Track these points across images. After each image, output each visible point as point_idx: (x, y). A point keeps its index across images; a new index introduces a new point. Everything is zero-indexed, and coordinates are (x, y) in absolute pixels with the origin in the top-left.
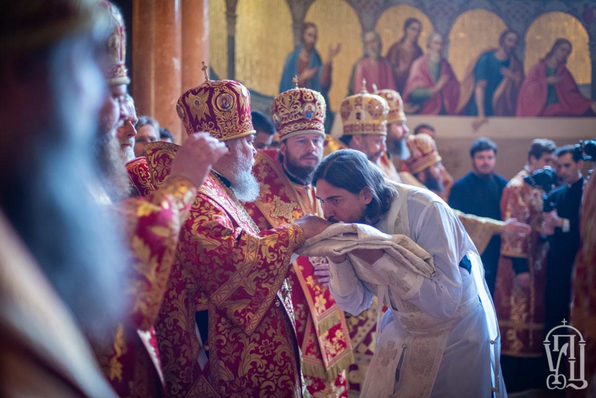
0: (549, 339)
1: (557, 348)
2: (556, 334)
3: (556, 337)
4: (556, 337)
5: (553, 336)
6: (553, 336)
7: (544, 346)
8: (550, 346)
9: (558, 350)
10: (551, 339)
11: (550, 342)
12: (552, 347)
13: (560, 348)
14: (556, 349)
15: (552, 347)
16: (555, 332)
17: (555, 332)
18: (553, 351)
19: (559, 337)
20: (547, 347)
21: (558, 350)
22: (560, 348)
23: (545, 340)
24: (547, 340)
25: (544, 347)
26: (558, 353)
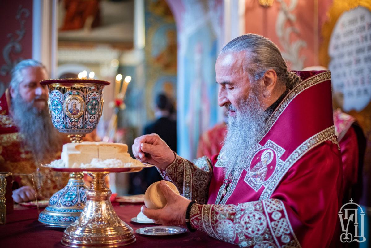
0: (342, 211)
1: (347, 217)
2: (346, 208)
3: (346, 210)
4: (346, 210)
5: (345, 209)
6: (345, 209)
7: (339, 215)
8: (342, 216)
9: (347, 218)
10: (343, 211)
11: (342, 213)
12: (343, 216)
13: (348, 217)
14: (346, 217)
15: (343, 216)
16: (346, 207)
17: (346, 207)
18: (344, 218)
19: (348, 210)
20: (341, 216)
21: (347, 218)
22: (348, 217)
23: (339, 211)
24: (340, 212)
25: (338, 216)
26: (347, 220)
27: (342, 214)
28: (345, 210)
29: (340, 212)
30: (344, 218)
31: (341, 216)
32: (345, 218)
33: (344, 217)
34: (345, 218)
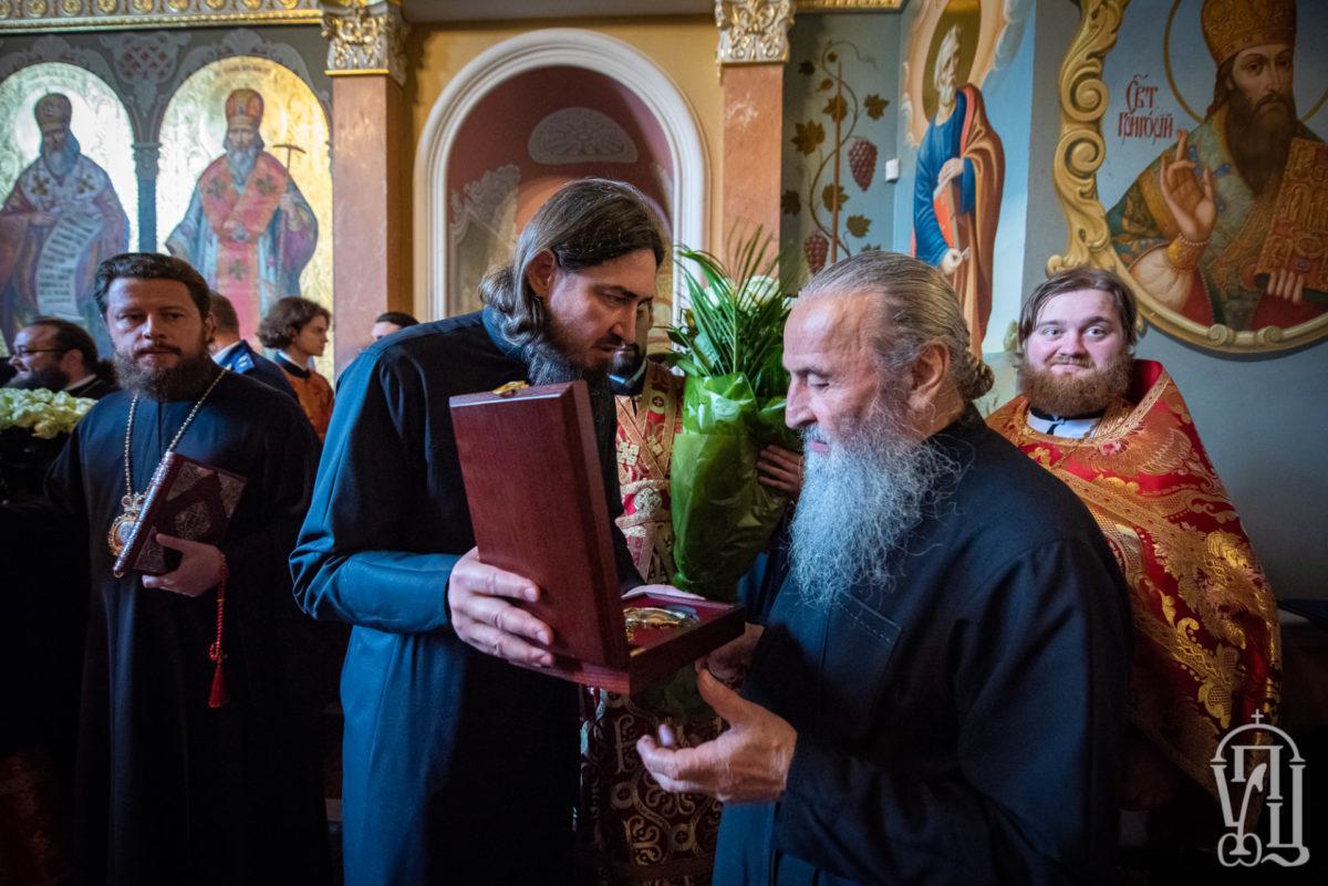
1: (1242, 774)
3: (1239, 751)
9: (1244, 780)
10: (1229, 755)
12: (1229, 773)
13: (1247, 774)
14: (1239, 777)
16: (1237, 740)
17: (1237, 740)
18: (1233, 780)
19: (1246, 751)
20: (1219, 772)
22: (1247, 774)
23: (1214, 756)
24: (1218, 758)
25: (1211, 772)
26: (1246, 783)
27: (1225, 766)
28: (1233, 751)
29: (1218, 758)
30: (1233, 780)
31: (1219, 772)
33: (1233, 776)
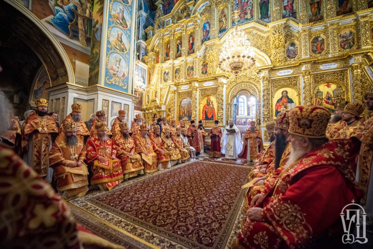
0: (344, 212)
3: (348, 211)
4: (348, 211)
9: (349, 219)
10: (345, 212)
12: (345, 217)
13: (350, 217)
14: (348, 218)
15: (345, 217)
16: (347, 208)
17: (347, 208)
21: (349, 219)
22: (350, 217)
32: (347, 219)
33: (346, 218)
34: (347, 219)
